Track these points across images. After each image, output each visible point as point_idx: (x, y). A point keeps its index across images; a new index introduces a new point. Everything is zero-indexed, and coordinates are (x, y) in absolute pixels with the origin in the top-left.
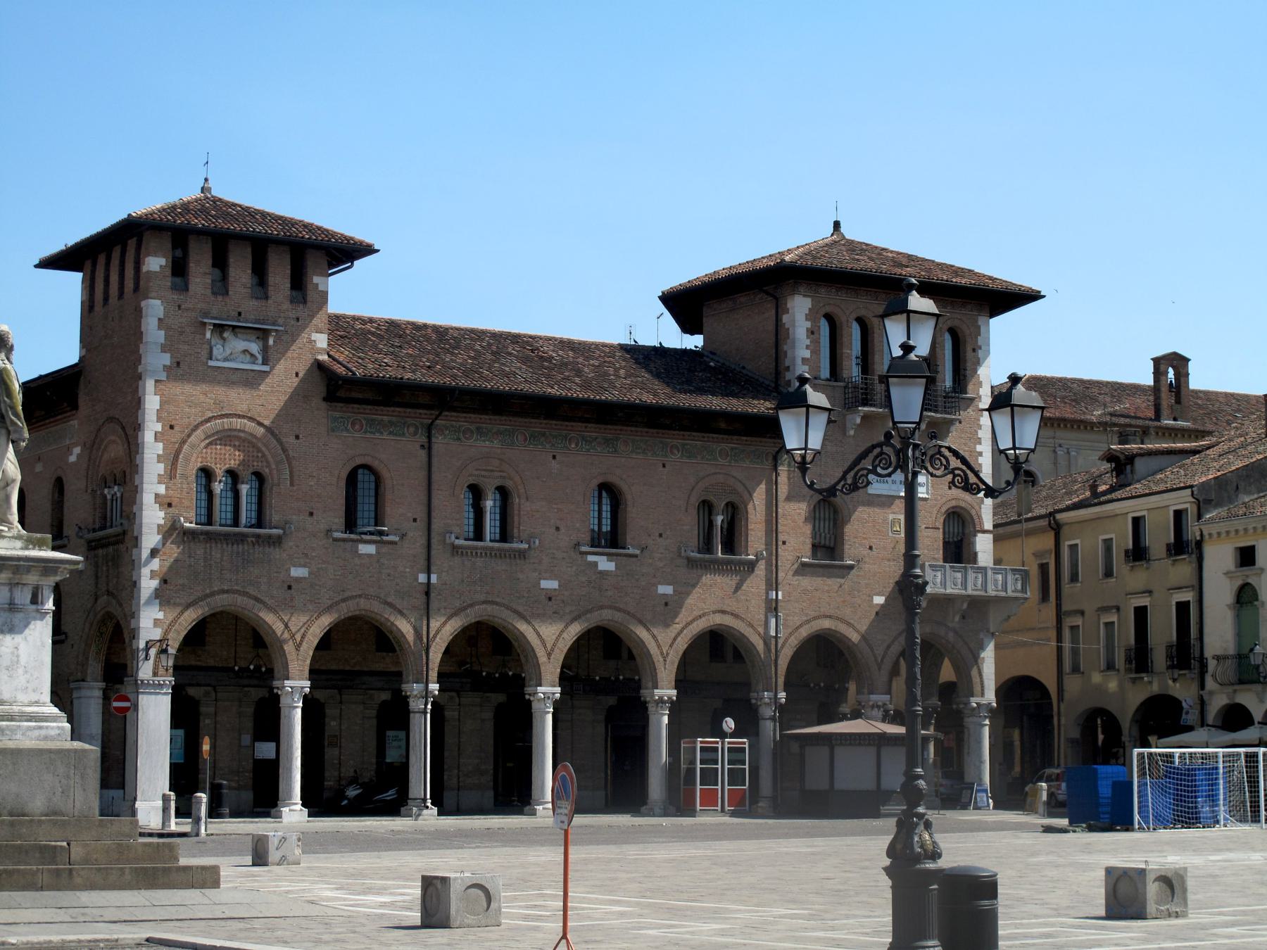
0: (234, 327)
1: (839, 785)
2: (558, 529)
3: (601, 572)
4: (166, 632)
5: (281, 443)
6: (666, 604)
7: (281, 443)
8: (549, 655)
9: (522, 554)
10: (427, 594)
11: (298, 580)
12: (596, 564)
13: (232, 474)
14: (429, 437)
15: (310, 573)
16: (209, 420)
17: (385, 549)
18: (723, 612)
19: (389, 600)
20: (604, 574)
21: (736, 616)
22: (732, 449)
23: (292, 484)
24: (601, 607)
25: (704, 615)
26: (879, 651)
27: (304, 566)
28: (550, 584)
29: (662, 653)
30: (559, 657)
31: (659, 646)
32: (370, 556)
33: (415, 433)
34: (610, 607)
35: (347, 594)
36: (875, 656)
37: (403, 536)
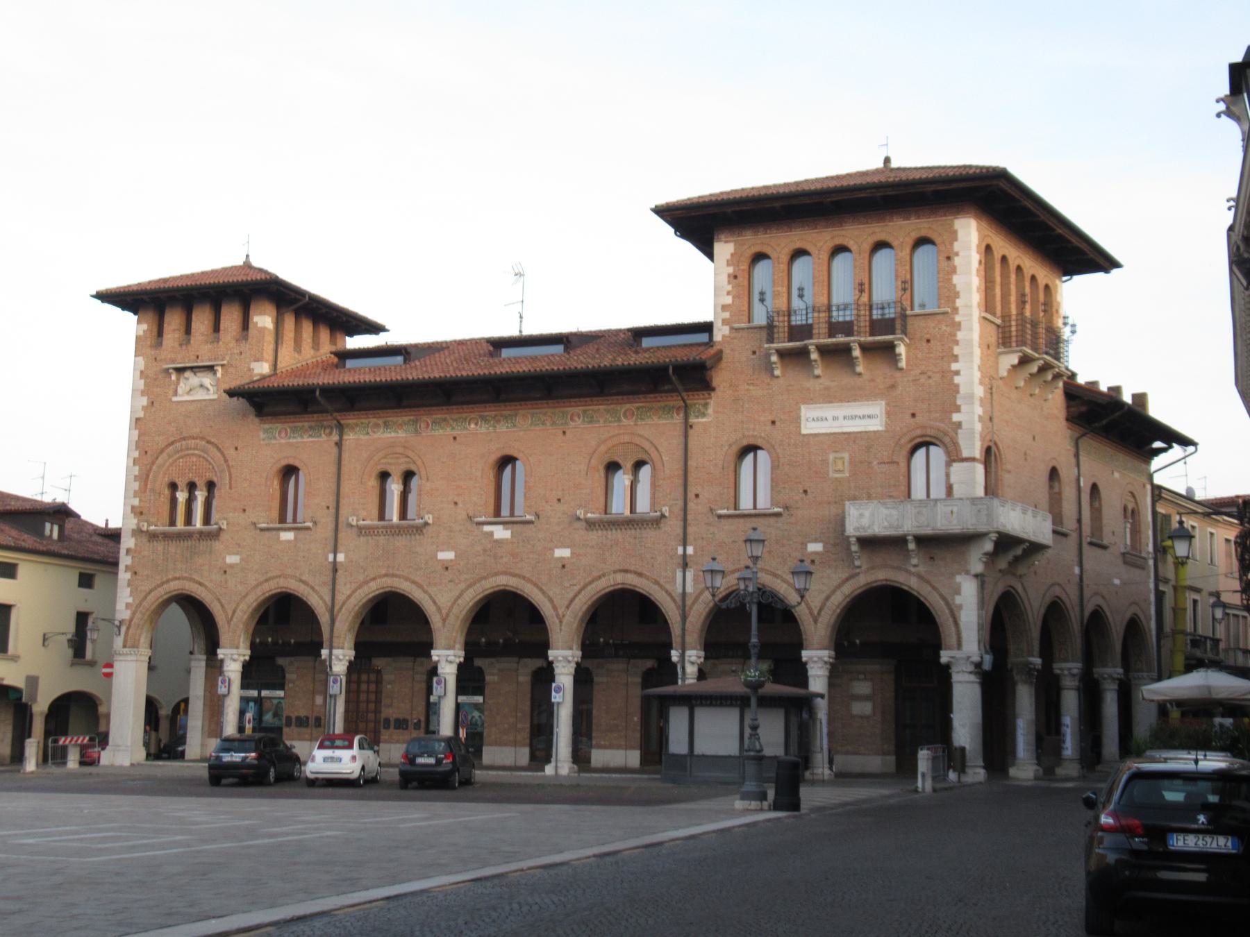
0: (192, 368)
1: (698, 750)
2: (456, 503)
3: (497, 541)
4: (134, 614)
5: (223, 454)
7: (223, 454)
8: (444, 620)
10: (335, 570)
11: (232, 566)
12: (491, 534)
13: (192, 487)
14: (341, 436)
15: (242, 560)
16: (172, 443)
17: (302, 535)
18: (626, 571)
19: (304, 578)
20: (500, 542)
21: (640, 575)
22: (638, 408)
23: (230, 488)
24: (496, 574)
25: (604, 575)
27: (237, 554)
28: (447, 555)
29: (557, 615)
30: (828, 617)
31: (555, 608)
32: (289, 542)
33: (330, 434)
34: (505, 573)
35: (269, 575)
37: (315, 523)
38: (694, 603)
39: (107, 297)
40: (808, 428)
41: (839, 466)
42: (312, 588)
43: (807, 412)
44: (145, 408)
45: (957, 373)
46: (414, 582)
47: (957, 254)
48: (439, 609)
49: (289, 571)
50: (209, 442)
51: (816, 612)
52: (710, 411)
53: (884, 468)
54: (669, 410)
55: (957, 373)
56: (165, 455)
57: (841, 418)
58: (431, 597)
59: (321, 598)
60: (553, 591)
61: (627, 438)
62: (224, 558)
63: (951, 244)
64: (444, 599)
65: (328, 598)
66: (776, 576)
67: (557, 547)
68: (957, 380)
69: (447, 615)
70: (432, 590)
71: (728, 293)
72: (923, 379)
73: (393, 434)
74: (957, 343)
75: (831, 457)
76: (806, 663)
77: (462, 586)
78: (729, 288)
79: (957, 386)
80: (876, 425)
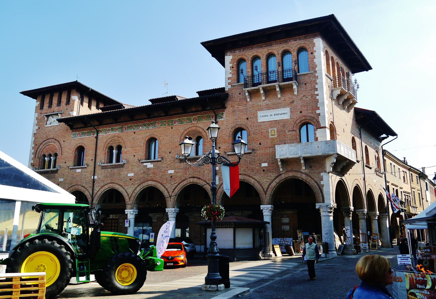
0: (51, 115)
2: (134, 156)
3: (148, 168)
5: (60, 144)
6: (171, 177)
7: (60, 144)
8: (130, 199)
9: (122, 166)
10: (94, 182)
16: (45, 141)
17: (84, 170)
18: (194, 177)
20: (149, 169)
21: (199, 178)
22: (198, 117)
24: (148, 181)
25: (186, 179)
26: (265, 187)
28: (131, 175)
31: (168, 192)
33: (94, 134)
34: (151, 180)
36: (263, 188)
37: (88, 165)
38: (219, 189)
39: (25, 93)
40: (260, 120)
41: (273, 133)
42: (86, 189)
43: (260, 114)
44: (37, 130)
45: (318, 95)
46: (120, 185)
47: (315, 51)
48: (128, 194)
49: (79, 183)
50: (56, 140)
51: (265, 190)
52: (224, 116)
53: (291, 132)
54: (209, 117)
55: (318, 95)
56: (42, 145)
57: (273, 115)
58: (125, 190)
59: (89, 193)
60: (168, 186)
61: (194, 128)
62: (58, 180)
63: (313, 48)
64: (130, 191)
65: (91, 192)
66: (250, 176)
67: (169, 170)
68: (317, 97)
69: (131, 196)
70: (126, 188)
71: (230, 73)
72: (304, 98)
73: (114, 133)
74: (317, 84)
75: (270, 130)
76: (262, 210)
77: (136, 186)
78: (231, 71)
79: (318, 100)
80: (287, 117)
